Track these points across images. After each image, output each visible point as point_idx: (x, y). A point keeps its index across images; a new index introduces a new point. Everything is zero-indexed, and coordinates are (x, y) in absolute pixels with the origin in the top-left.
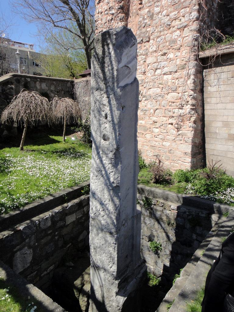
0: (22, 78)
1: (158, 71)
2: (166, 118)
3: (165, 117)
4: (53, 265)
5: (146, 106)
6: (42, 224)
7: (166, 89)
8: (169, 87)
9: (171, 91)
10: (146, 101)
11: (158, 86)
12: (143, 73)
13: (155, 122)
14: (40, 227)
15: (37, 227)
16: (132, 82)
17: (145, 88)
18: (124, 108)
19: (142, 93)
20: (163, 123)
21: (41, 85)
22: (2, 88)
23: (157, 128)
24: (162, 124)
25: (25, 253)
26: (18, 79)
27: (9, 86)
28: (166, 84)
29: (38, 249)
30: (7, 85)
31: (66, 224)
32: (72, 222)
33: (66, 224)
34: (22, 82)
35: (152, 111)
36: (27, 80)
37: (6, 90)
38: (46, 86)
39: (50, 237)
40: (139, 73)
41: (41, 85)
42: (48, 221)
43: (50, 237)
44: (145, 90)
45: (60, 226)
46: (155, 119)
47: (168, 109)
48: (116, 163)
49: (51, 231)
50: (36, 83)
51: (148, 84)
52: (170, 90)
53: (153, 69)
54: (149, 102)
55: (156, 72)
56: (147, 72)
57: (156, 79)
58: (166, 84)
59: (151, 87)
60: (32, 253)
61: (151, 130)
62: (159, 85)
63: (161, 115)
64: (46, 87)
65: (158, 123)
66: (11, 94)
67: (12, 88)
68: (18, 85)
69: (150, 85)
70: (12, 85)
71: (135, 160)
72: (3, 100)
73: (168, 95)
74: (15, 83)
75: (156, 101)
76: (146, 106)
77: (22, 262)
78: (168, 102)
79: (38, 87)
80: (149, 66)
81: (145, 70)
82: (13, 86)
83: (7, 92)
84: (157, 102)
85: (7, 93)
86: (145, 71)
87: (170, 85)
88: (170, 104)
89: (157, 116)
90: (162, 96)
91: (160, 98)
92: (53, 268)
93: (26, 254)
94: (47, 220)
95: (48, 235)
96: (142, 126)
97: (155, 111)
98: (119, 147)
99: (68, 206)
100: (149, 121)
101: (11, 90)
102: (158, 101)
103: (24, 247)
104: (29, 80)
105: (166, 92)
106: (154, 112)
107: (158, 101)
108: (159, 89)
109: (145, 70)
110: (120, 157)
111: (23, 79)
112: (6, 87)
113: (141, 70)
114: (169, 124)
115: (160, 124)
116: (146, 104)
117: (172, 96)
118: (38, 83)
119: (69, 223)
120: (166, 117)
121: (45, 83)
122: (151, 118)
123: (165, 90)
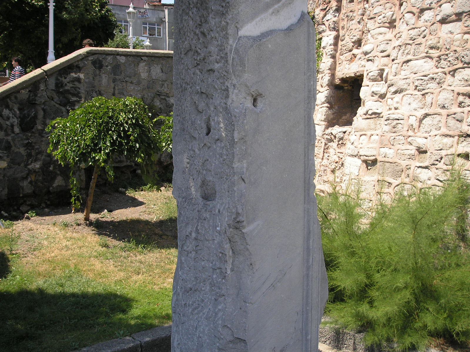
0: (107, 57)
1: (428, 15)
2: (451, 139)
3: (446, 136)
5: (396, 109)
7: (448, 59)
8: (457, 55)
9: (460, 65)
10: (397, 95)
11: (427, 53)
12: (389, 23)
13: (422, 151)
16: (292, 25)
17: (393, 60)
18: (259, 100)
19: (387, 74)
20: (443, 153)
21: (149, 71)
22: (57, 79)
23: (426, 168)
24: (438, 158)
26: (100, 61)
27: (73, 75)
28: (448, 47)
30: (67, 74)
34: (107, 66)
35: (413, 121)
36: (120, 61)
37: (66, 85)
38: (162, 72)
40: (379, 25)
41: (149, 71)
44: (395, 66)
46: (420, 142)
47: (455, 114)
48: (235, 269)
50: (138, 64)
51: (401, 51)
52: (459, 61)
53: (415, 10)
54: (405, 98)
55: (422, 17)
56: (398, 20)
57: (422, 36)
58: (448, 47)
59: (409, 57)
61: (410, 172)
62: (431, 51)
63: (437, 132)
64: (161, 74)
65: (428, 154)
66: (76, 92)
67: (78, 80)
68: (98, 72)
69: (406, 52)
70: (80, 72)
71: (308, 261)
72: (57, 106)
73: (453, 76)
74: (91, 68)
75: (422, 93)
76: (396, 109)
78: (456, 95)
79: (144, 75)
80: (404, 3)
81: (393, 15)
82: (82, 76)
83: (66, 88)
84: (427, 96)
85: (68, 91)
86: (394, 17)
87: (458, 49)
88: (461, 98)
89: (426, 135)
90: (437, 80)
91: (433, 85)
96: (387, 164)
97: (421, 121)
98: (240, 218)
100: (403, 147)
101: (76, 83)
102: (427, 93)
104: (122, 59)
105: (447, 70)
106: (418, 124)
107: (427, 93)
108: (429, 60)
109: (393, 15)
110: (248, 250)
111: (109, 58)
112: (65, 78)
113: (383, 15)
114: (459, 155)
115: (434, 158)
116: (397, 102)
117: (466, 78)
118: (142, 65)
120: (450, 136)
121: (160, 66)
122: (409, 139)
123: (445, 62)
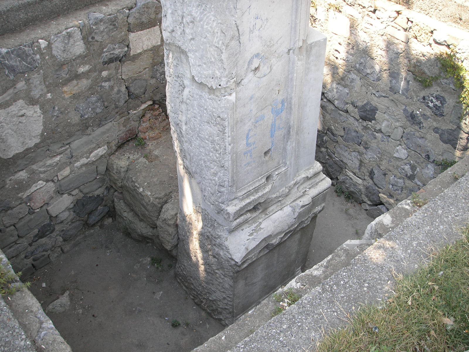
4: (104, 146)
6: (57, 47)
14: (52, 56)
15: (42, 54)
25: (20, 114)
29: (56, 109)
31: (132, 53)
32: (149, 48)
33: (132, 53)
39: (85, 83)
42: (75, 42)
43: (85, 83)
45: (112, 56)
49: (87, 68)
60: (40, 116)
77: (15, 132)
92: (104, 152)
93: (23, 116)
94: (71, 40)
95: (77, 77)
99: (136, 4)
103: (14, 100)
119: (139, 51)
